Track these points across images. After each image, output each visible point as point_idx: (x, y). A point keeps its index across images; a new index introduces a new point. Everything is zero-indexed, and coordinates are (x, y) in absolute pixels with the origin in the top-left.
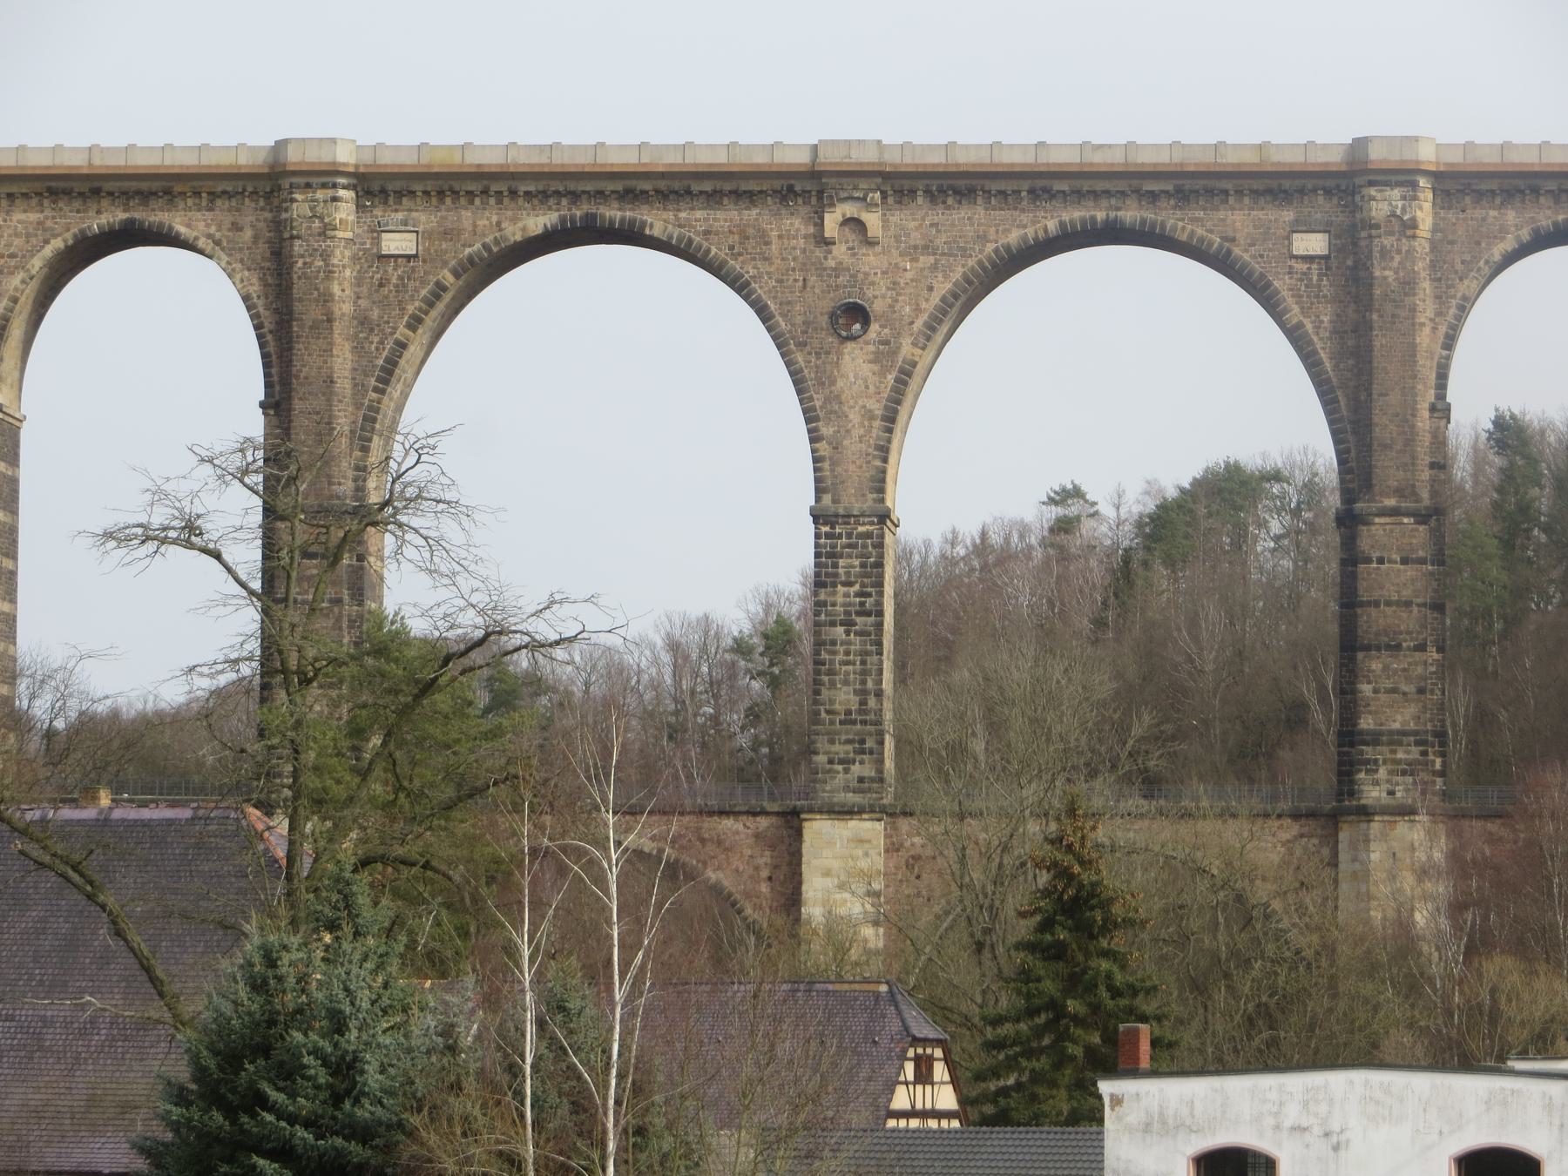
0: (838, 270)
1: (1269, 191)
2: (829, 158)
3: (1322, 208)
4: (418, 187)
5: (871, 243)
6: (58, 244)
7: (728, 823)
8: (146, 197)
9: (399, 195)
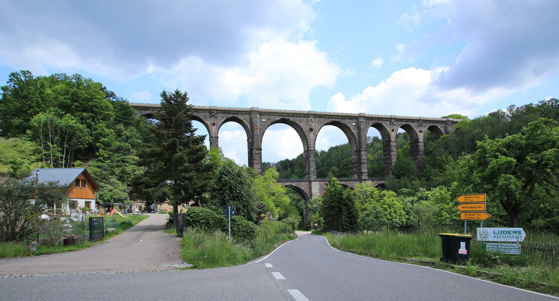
0: (309, 125)
2: (310, 113)
3: (355, 120)
4: (266, 114)
5: (313, 122)
6: (225, 119)
7: (303, 183)
8: (235, 114)
9: (264, 115)
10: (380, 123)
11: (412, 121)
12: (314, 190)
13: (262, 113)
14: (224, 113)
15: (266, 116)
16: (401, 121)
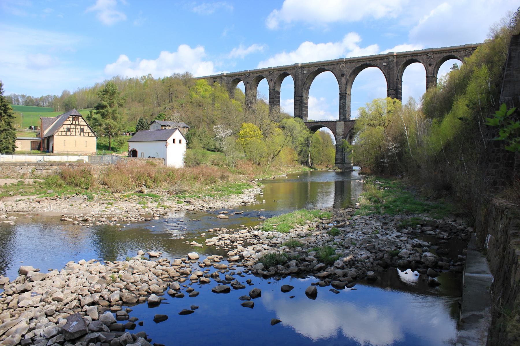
1: (380, 59)
3: (386, 60)
10: (414, 59)
11: (457, 51)
12: (338, 130)
13: (304, 67)
14: (278, 70)
15: (307, 69)
16: (442, 53)
